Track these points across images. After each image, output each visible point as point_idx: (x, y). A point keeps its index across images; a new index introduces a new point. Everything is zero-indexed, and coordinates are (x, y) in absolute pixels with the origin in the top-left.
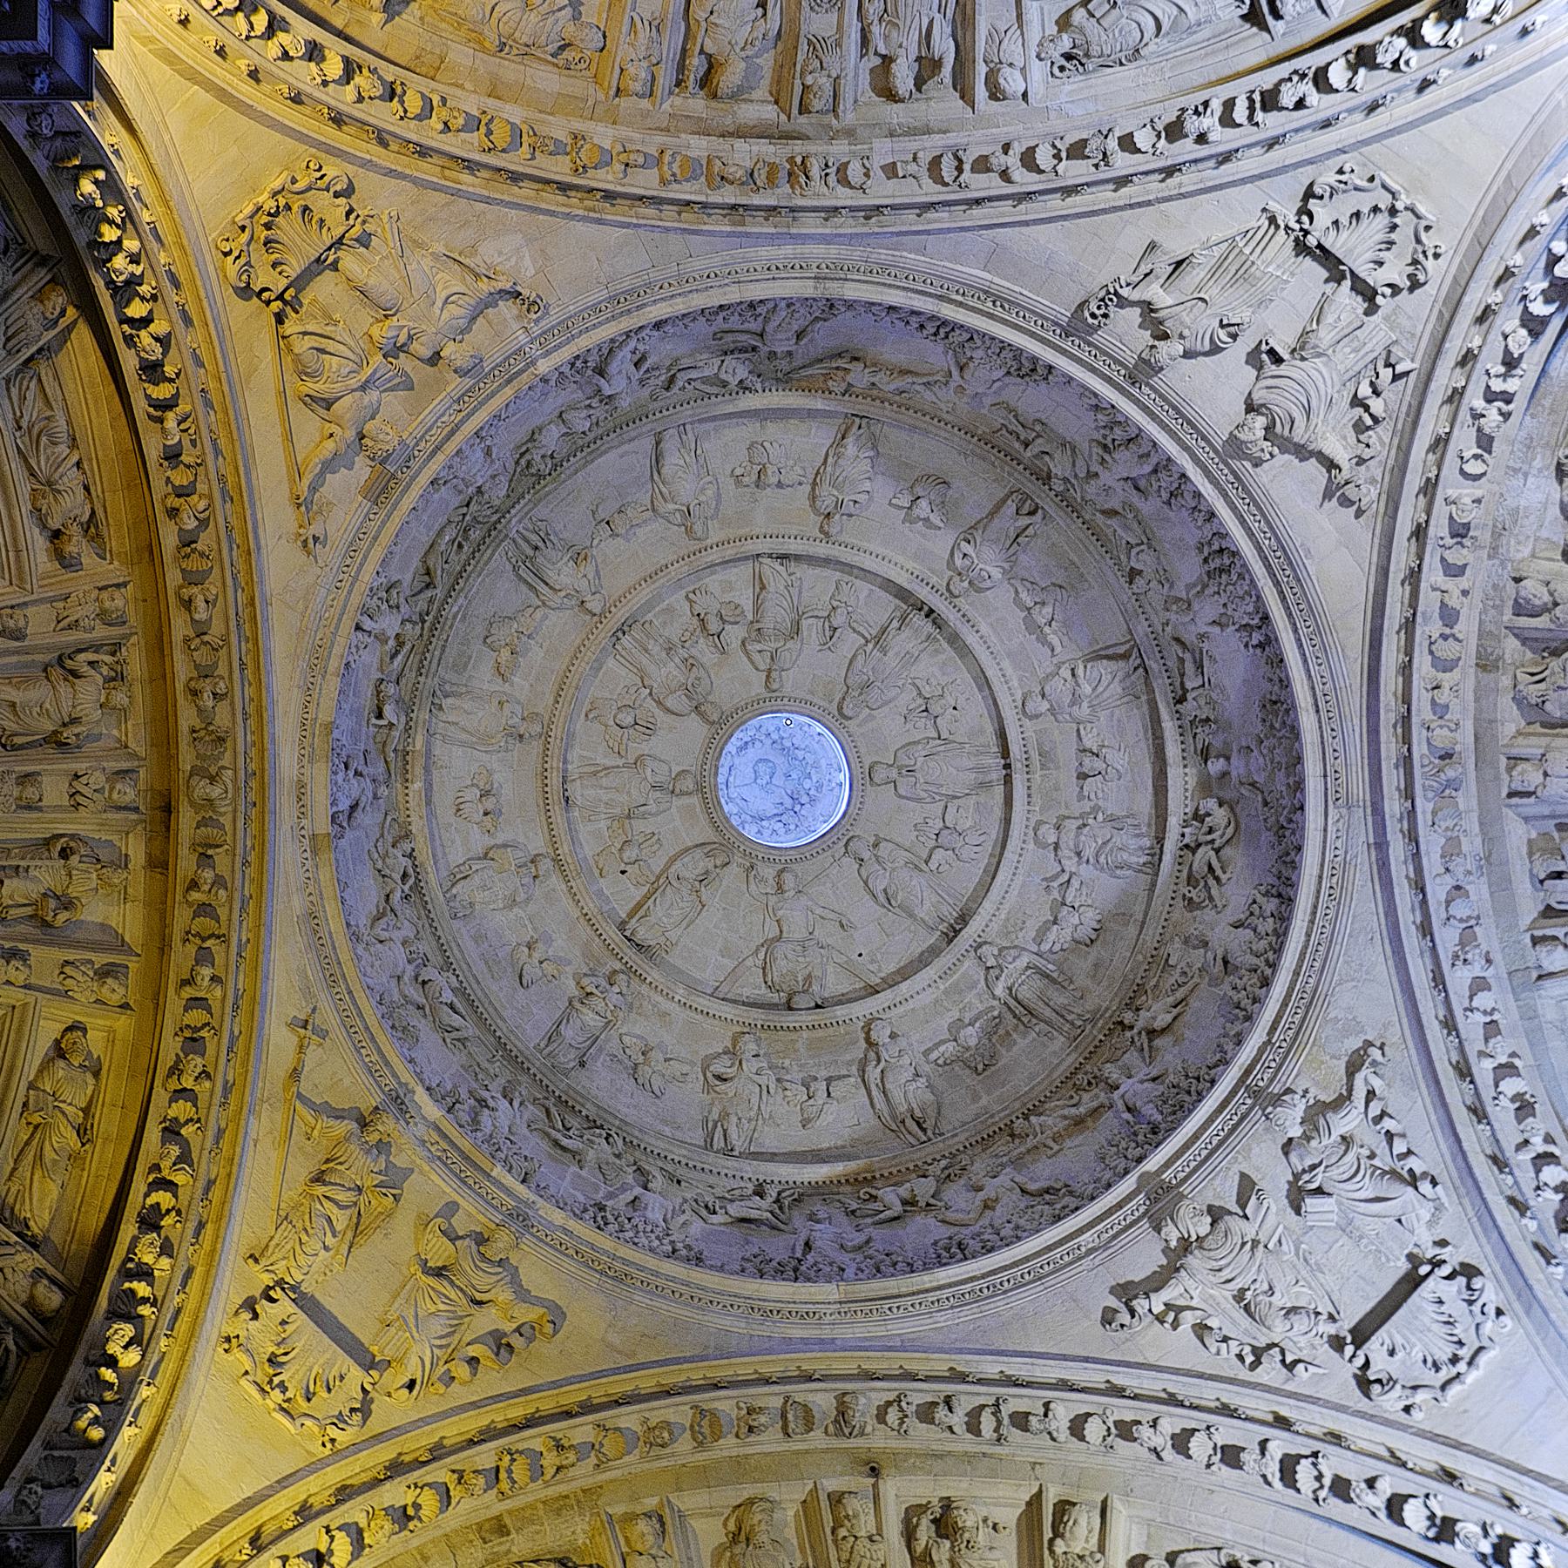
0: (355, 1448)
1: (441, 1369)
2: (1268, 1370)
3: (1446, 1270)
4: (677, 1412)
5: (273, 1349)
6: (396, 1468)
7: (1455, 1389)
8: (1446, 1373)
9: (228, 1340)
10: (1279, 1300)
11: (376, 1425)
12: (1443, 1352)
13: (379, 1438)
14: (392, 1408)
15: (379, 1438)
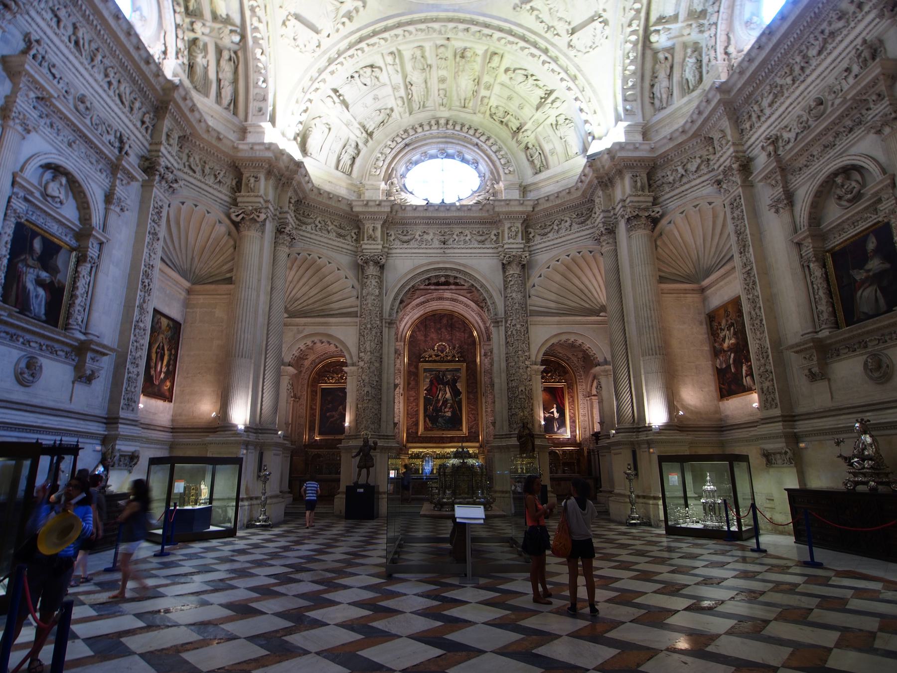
0: (320, 57)
1: (336, 28)
2: (549, 35)
3: (601, 20)
4: (399, 31)
5: (293, 35)
6: (331, 62)
7: (587, 54)
8: (587, 50)
9: (282, 36)
10: (559, 15)
11: (323, 48)
12: (590, 44)
13: (324, 53)
14: (326, 43)
15: (324, 53)
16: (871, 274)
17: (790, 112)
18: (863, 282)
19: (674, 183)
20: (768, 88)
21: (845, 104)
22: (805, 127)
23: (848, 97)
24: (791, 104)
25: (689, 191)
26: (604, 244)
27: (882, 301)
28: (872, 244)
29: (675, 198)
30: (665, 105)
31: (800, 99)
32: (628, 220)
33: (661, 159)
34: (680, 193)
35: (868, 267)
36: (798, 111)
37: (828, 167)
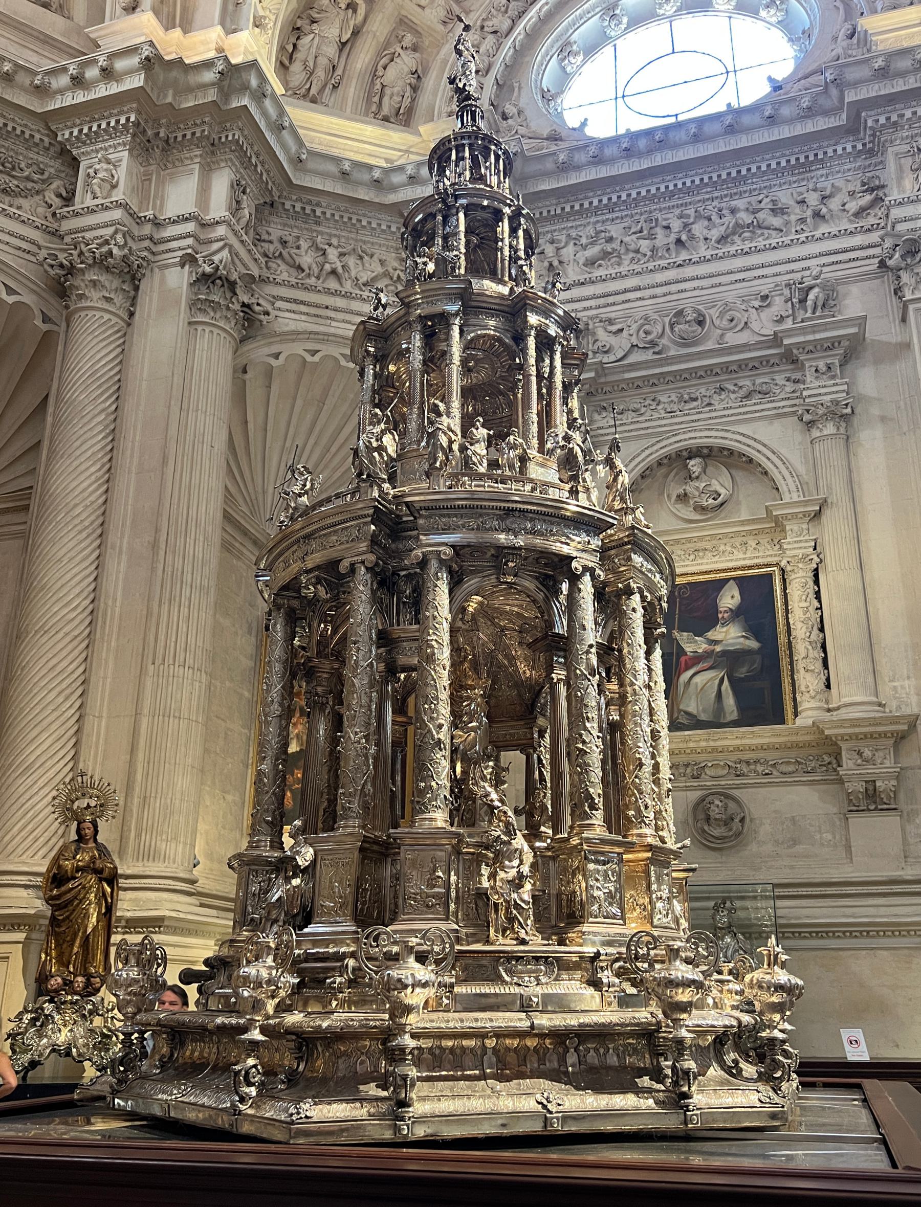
16: (718, 648)
17: (629, 301)
18: (697, 659)
19: (309, 275)
20: (590, 230)
21: (770, 347)
22: (653, 344)
23: (786, 342)
24: (639, 289)
25: (340, 316)
26: (95, 295)
27: (730, 701)
28: (730, 599)
29: (303, 308)
30: (313, 91)
31: (659, 291)
32: (206, 280)
33: (300, 200)
34: (317, 306)
35: (711, 635)
36: (647, 307)
37: (692, 435)
